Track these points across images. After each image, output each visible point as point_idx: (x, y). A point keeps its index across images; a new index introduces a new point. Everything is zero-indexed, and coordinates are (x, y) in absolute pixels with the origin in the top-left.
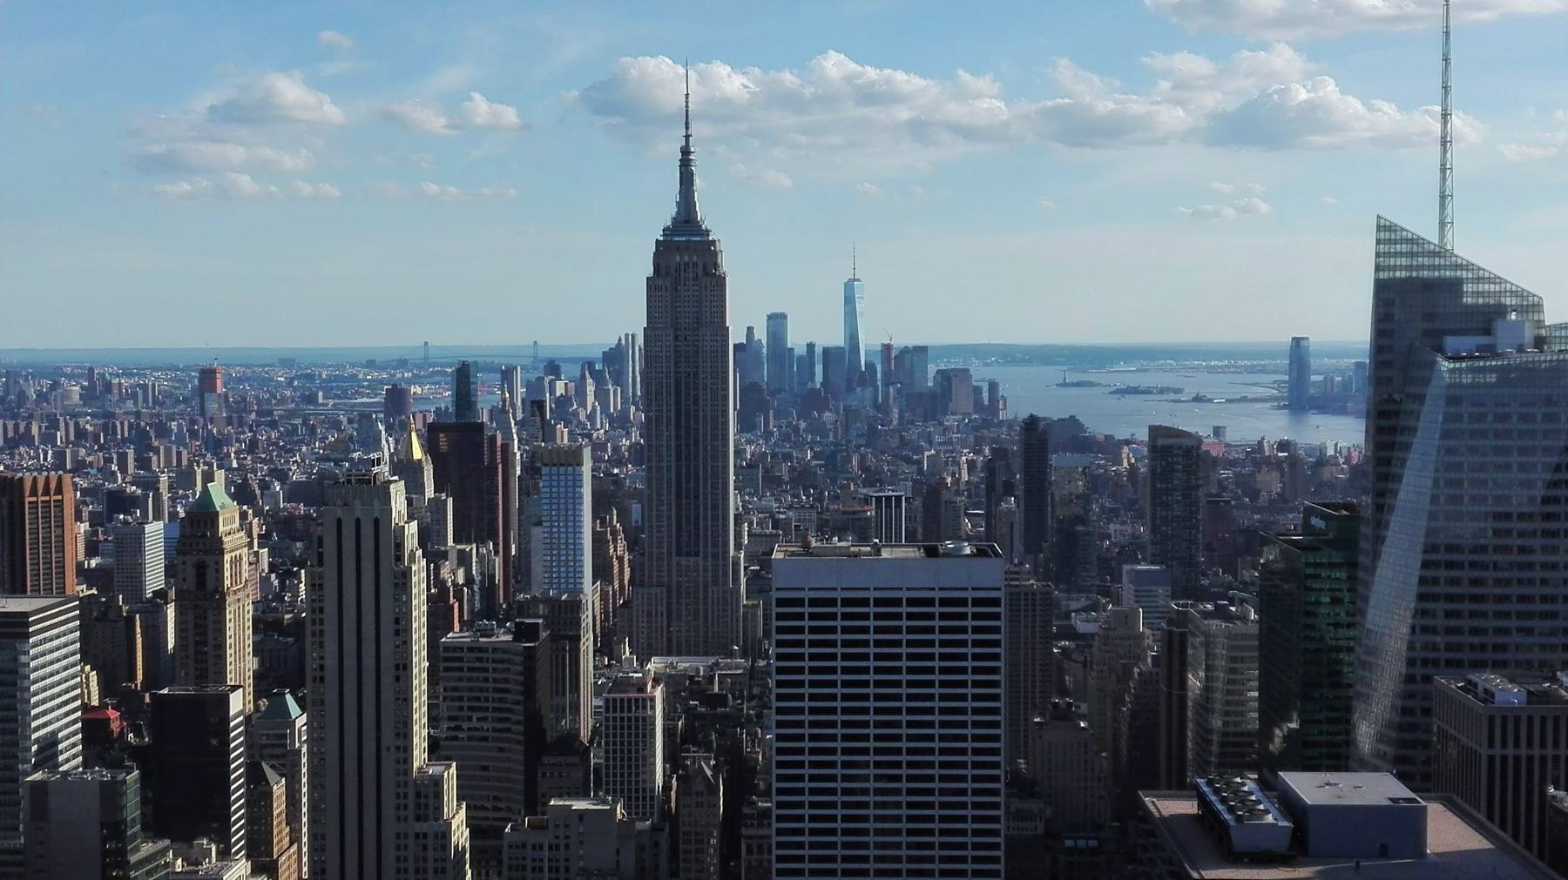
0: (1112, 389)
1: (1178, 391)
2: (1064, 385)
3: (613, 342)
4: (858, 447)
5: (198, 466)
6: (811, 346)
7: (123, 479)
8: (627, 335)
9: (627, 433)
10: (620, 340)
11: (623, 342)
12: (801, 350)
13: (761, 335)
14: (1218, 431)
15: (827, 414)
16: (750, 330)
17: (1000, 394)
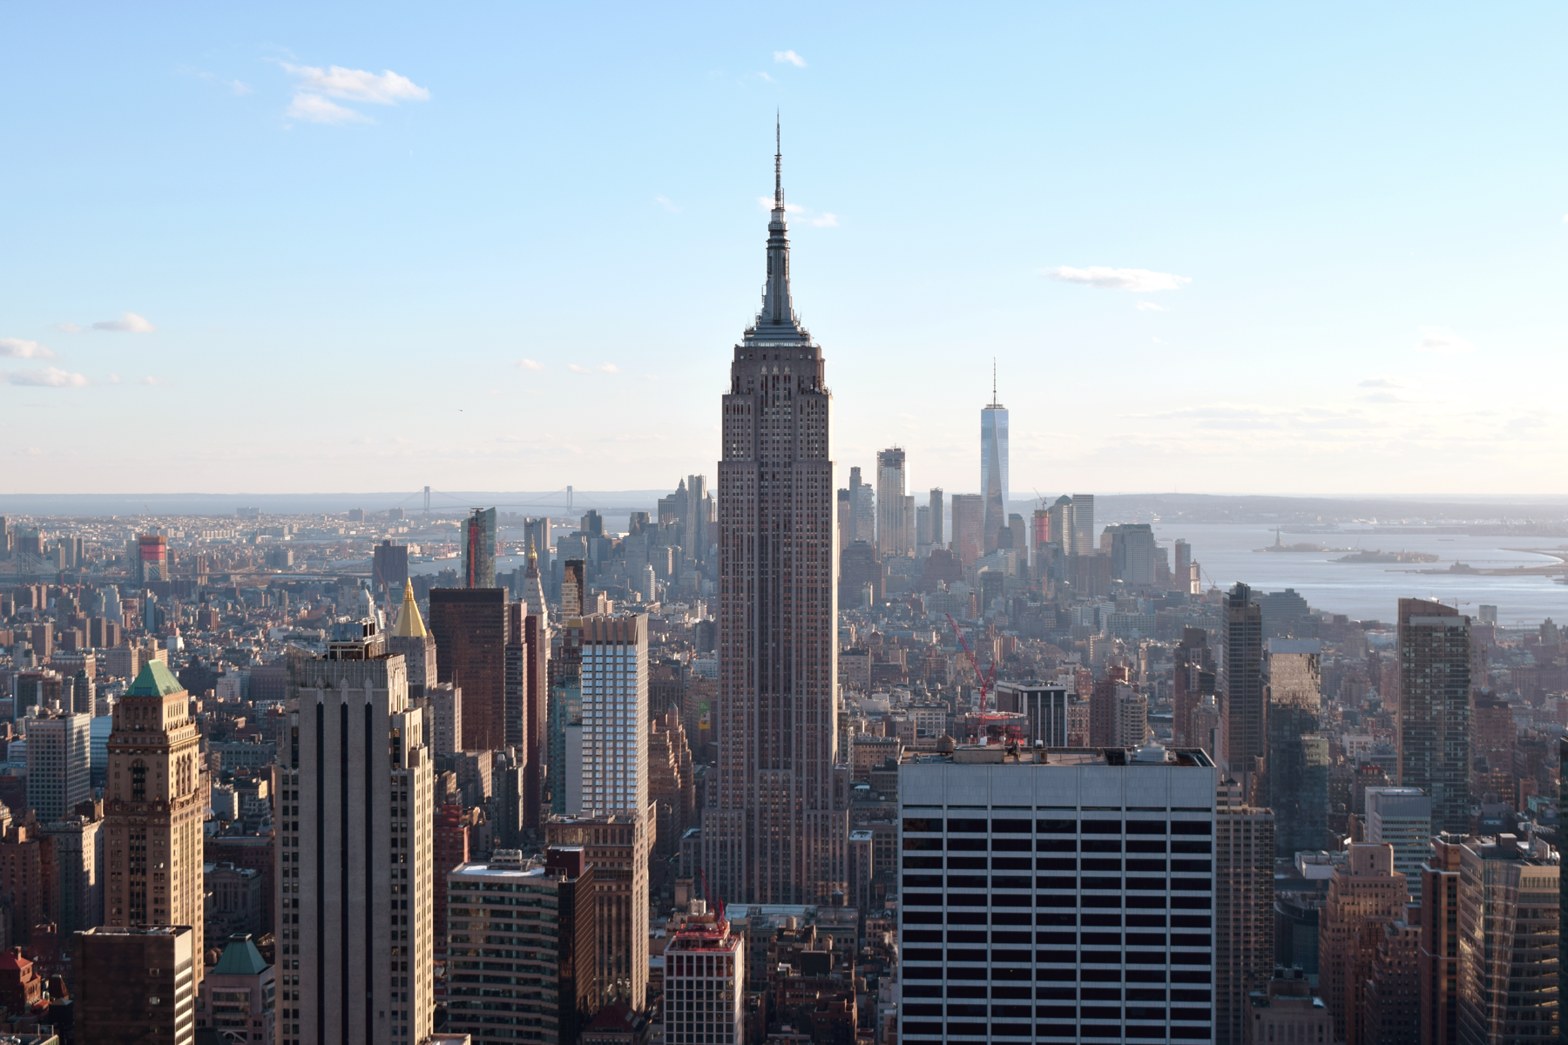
0: (1344, 555)
1: (1432, 558)
2: (1277, 548)
3: (676, 487)
4: (1001, 629)
5: (135, 645)
6: (936, 495)
7: (40, 660)
8: (691, 478)
9: (691, 608)
10: (682, 484)
11: (687, 487)
12: (923, 500)
13: (870, 477)
14: (1489, 611)
15: (959, 584)
16: (855, 471)
17: (1192, 560)
